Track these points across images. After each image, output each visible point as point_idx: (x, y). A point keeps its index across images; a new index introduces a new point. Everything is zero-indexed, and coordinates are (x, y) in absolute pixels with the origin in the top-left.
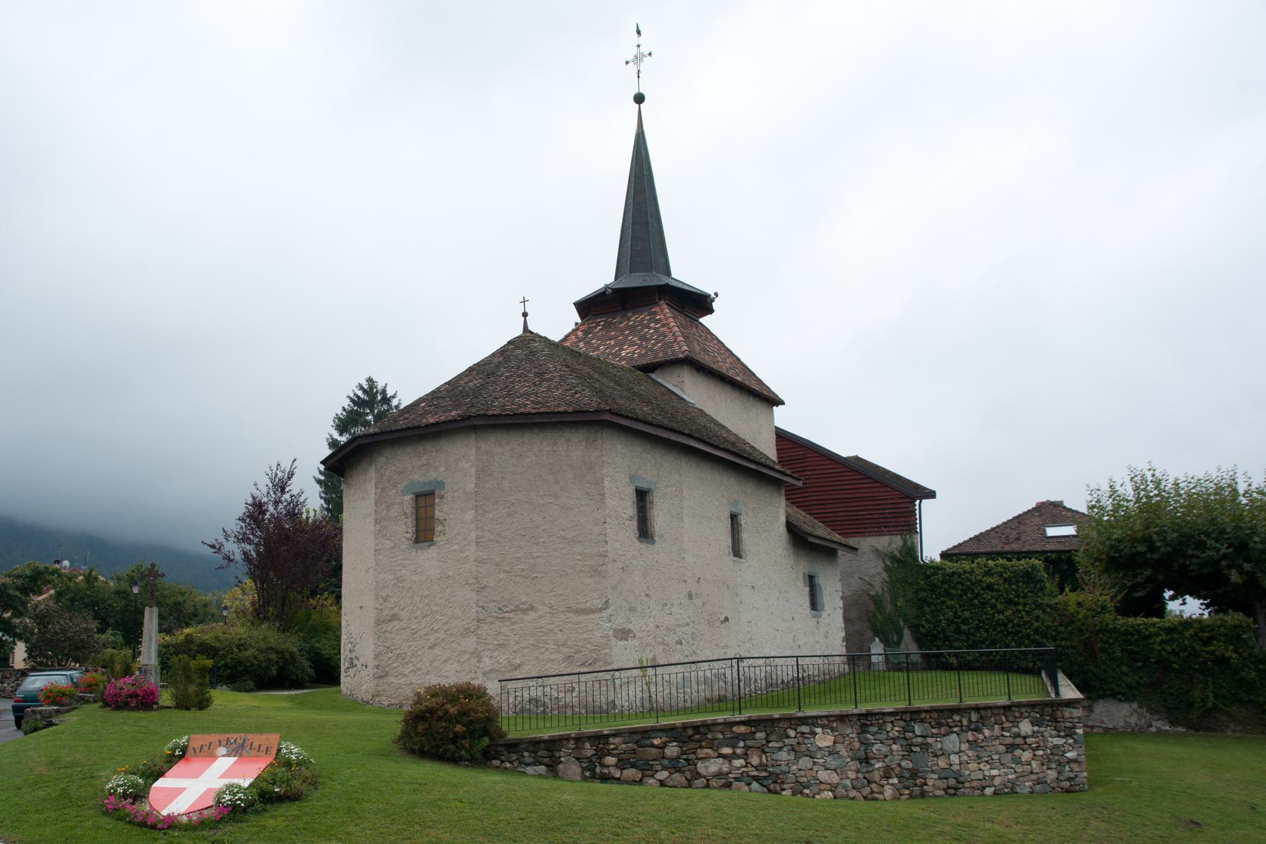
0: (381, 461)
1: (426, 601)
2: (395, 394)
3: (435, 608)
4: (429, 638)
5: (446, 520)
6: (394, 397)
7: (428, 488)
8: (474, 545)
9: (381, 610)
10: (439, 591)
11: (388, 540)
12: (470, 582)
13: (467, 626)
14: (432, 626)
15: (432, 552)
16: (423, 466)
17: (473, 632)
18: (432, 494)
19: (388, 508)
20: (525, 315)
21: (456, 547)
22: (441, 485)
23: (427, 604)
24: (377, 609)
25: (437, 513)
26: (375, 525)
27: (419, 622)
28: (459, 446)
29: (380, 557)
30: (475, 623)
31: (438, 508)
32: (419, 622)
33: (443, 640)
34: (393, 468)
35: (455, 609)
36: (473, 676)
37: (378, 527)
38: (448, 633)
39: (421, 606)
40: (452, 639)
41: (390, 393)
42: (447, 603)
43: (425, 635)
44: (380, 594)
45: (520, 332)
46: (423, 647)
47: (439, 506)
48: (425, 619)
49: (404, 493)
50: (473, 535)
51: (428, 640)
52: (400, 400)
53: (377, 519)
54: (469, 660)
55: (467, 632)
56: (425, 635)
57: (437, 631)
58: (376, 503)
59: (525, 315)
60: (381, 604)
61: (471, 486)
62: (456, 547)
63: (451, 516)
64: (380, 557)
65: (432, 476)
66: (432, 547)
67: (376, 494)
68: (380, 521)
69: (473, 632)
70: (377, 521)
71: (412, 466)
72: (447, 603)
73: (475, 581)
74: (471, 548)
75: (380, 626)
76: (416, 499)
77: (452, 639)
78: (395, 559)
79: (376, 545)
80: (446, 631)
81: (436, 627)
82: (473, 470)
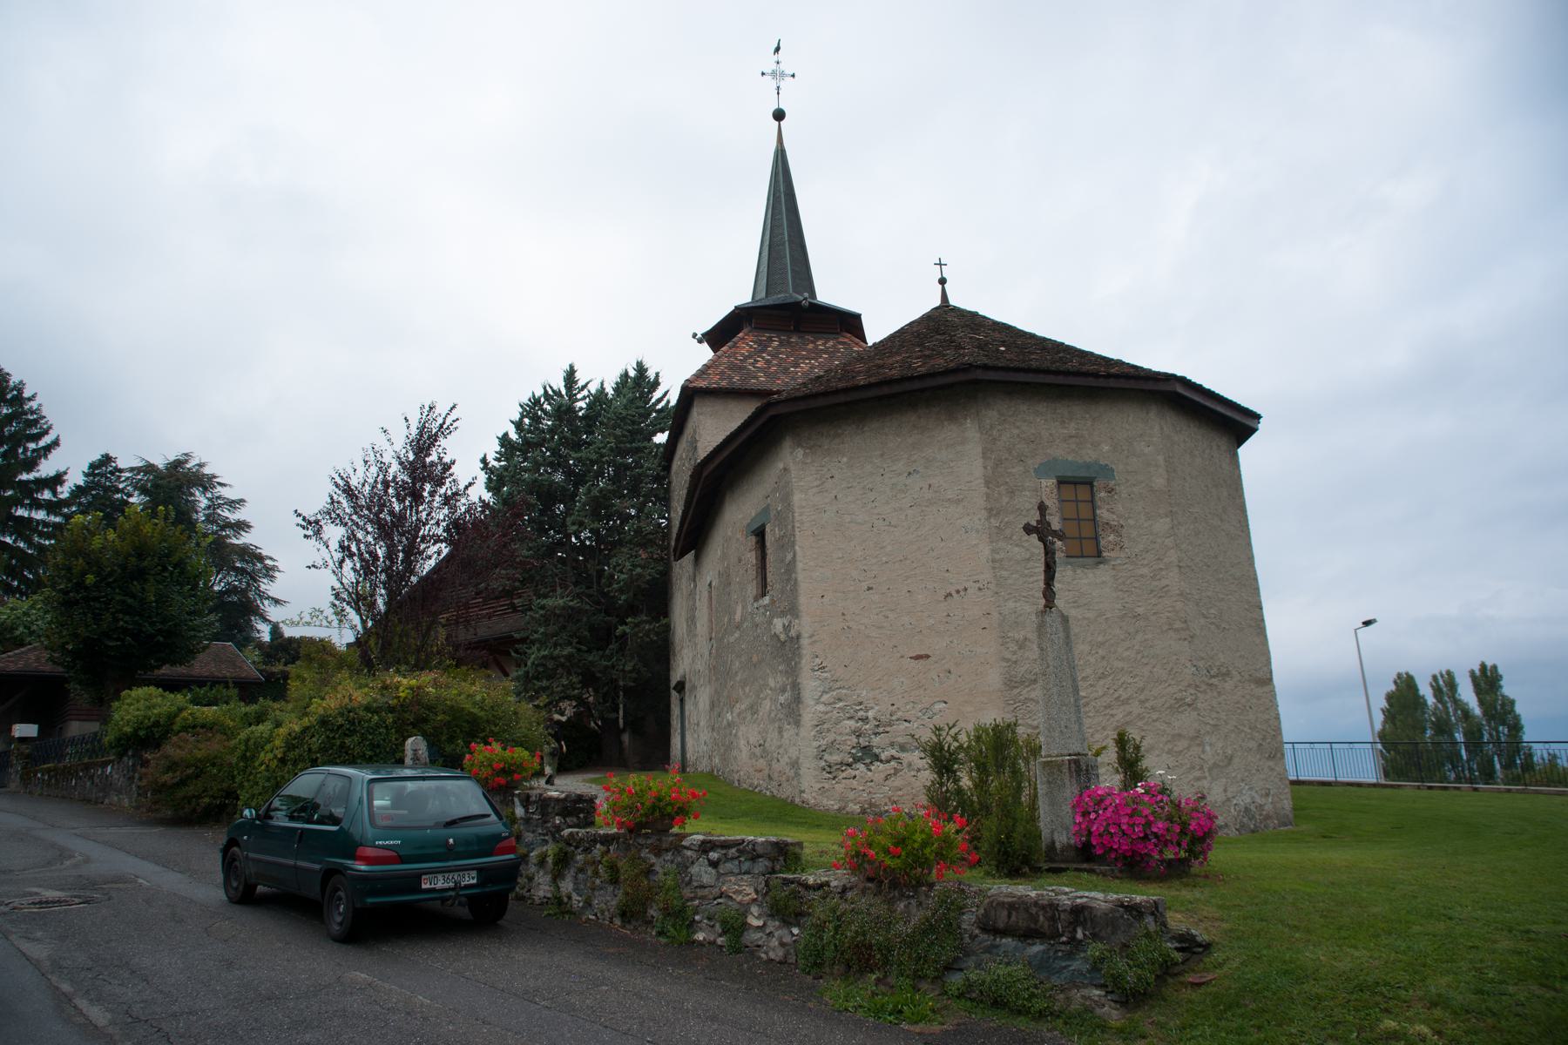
0: (991, 415)
1: (1101, 652)
2: (33, 396)
3: (1120, 664)
4: (1111, 712)
5: (1122, 526)
6: (30, 399)
7: (1083, 473)
8: (1176, 570)
9: (1016, 662)
10: (1122, 637)
11: (1017, 545)
12: (1176, 626)
13: (1179, 695)
14: (1116, 695)
15: (1103, 574)
16: (1071, 437)
17: (1189, 705)
18: (1089, 483)
19: (1012, 493)
20: (943, 281)
21: (1145, 571)
22: (1107, 471)
23: (1103, 658)
24: (1008, 660)
25: (1103, 514)
26: (988, 519)
27: (1091, 686)
28: (1130, 419)
29: (1005, 573)
30: (1193, 691)
31: (1106, 507)
32: (1091, 686)
33: (1140, 717)
34: (1016, 431)
35: (1154, 667)
36: (1198, 774)
37: (994, 522)
38: (1147, 705)
39: (1092, 660)
40: (1155, 716)
41: (26, 394)
42: (1139, 656)
43: (1106, 707)
44: (1010, 634)
45: (937, 303)
46: (1104, 728)
47: (1108, 504)
48: (1102, 682)
49: (1041, 472)
50: (1173, 556)
51: (1112, 715)
52: (40, 405)
53: (991, 509)
54: (1188, 748)
55: (1180, 705)
56: (1106, 707)
57: (1126, 702)
58: (987, 483)
59: (943, 281)
60: (1014, 653)
61: (1159, 482)
62: (1145, 571)
63: (1131, 522)
64: (1005, 573)
65: (1089, 455)
66: (1102, 566)
67: (985, 468)
68: (998, 513)
69: (1189, 705)
70: (992, 512)
71: (1051, 434)
72: (1139, 656)
73: (1183, 625)
74: (1171, 574)
75: (1016, 691)
76: (1059, 487)
77: (1155, 716)
78: (1031, 579)
79: (993, 551)
80: (1142, 702)
81: (1125, 696)
82: (1161, 458)
